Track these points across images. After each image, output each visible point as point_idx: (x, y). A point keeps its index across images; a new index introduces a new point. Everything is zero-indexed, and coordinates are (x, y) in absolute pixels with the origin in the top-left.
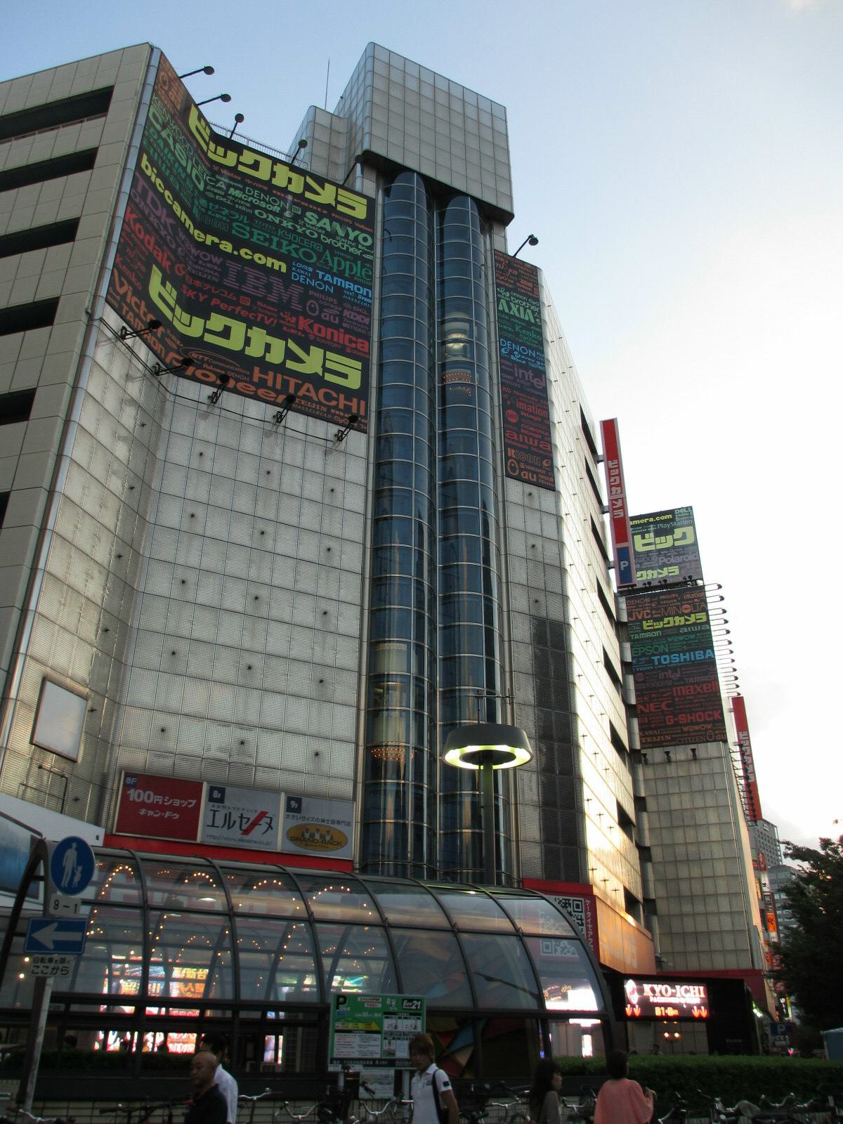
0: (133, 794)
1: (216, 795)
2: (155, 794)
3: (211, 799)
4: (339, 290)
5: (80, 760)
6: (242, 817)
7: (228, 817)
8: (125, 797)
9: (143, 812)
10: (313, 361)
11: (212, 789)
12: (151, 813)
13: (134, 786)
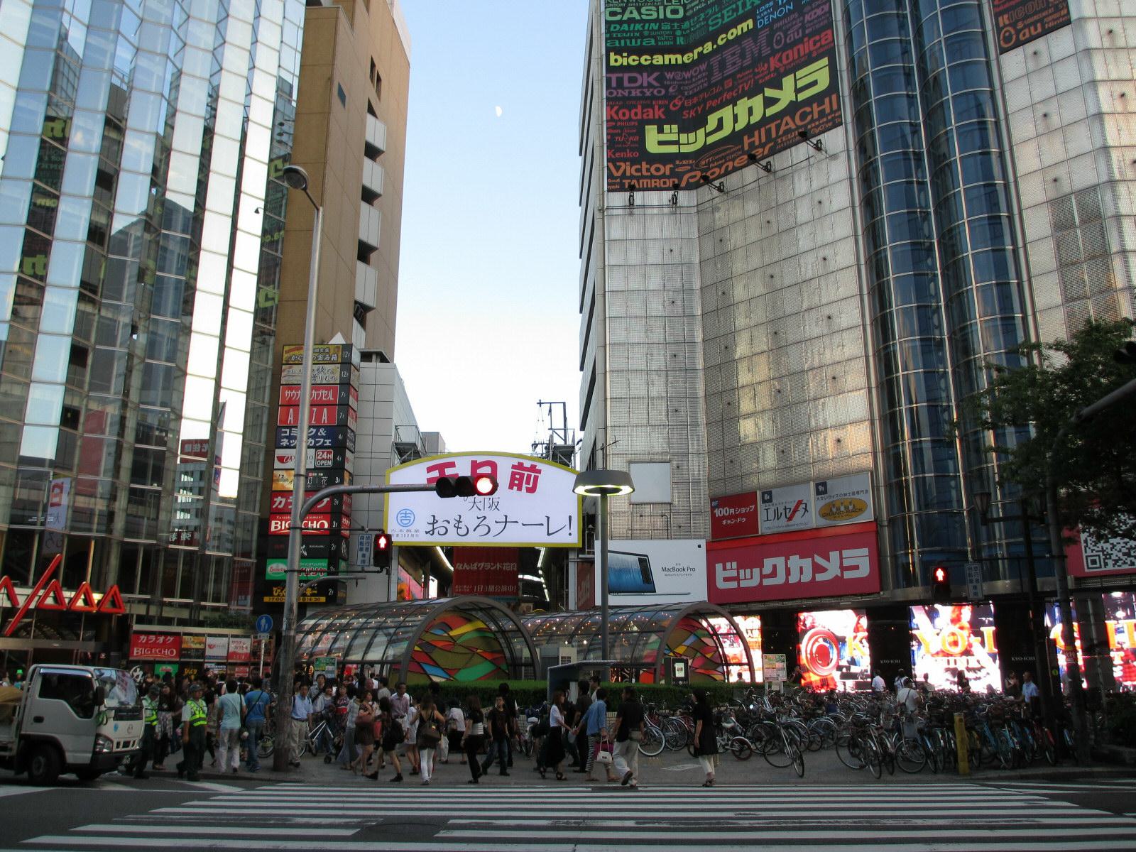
0: (717, 512)
1: (767, 497)
3: (764, 501)
5: (676, 502)
6: (785, 509)
7: (776, 511)
8: (713, 515)
11: (763, 494)
13: (718, 506)
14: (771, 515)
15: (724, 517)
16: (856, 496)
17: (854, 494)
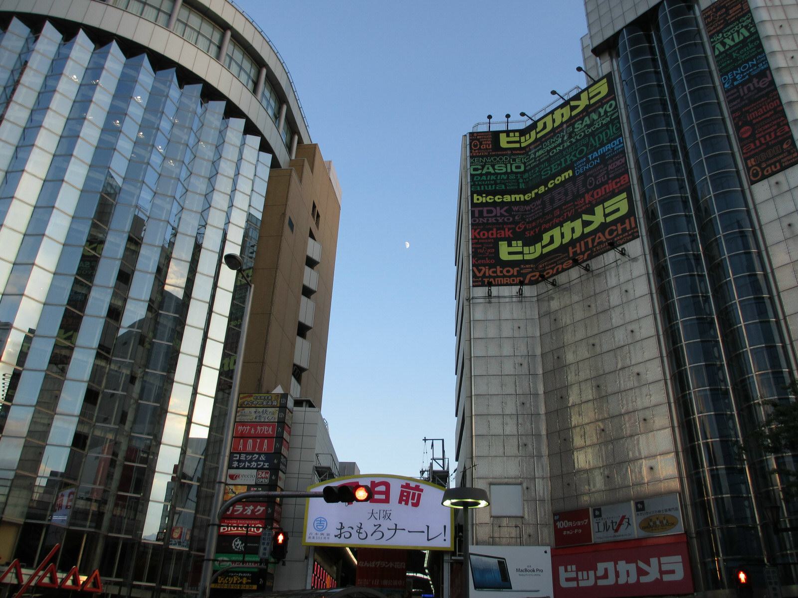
0: (559, 524)
1: (597, 513)
2: (568, 521)
3: (595, 516)
4: (603, 156)
6: (612, 522)
7: (605, 525)
8: (555, 526)
9: (565, 533)
10: (598, 218)
11: (594, 510)
12: (568, 532)
13: (559, 520)
14: (602, 528)
15: (564, 529)
16: (669, 513)
17: (666, 510)
